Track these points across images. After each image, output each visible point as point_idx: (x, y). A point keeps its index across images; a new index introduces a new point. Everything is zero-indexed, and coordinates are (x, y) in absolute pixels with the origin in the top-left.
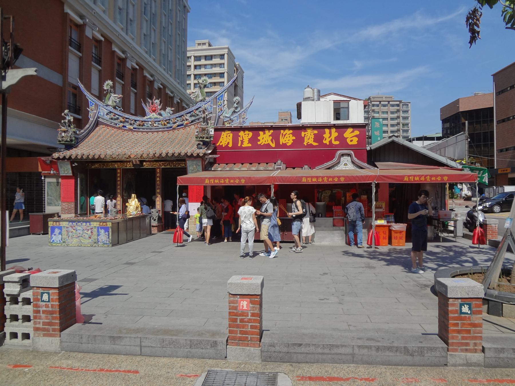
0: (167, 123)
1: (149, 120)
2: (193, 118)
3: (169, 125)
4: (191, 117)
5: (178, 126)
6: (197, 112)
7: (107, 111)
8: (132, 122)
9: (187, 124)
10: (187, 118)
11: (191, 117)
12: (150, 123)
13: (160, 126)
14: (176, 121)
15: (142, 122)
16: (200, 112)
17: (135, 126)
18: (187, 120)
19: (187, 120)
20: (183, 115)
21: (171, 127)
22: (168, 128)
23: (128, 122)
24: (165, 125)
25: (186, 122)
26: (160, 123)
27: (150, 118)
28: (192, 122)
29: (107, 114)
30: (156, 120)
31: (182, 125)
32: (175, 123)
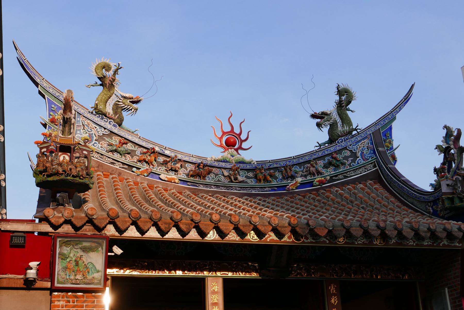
0: (271, 176)
1: (223, 165)
2: (331, 171)
3: (274, 183)
4: (326, 167)
5: (303, 185)
6: (340, 157)
7: (101, 132)
8: (178, 165)
9: (321, 182)
10: (320, 169)
11: (326, 167)
12: (226, 173)
13: (252, 182)
14: (293, 173)
15: (205, 165)
16: (346, 158)
17: (184, 177)
18: (319, 173)
19: (319, 173)
20: (308, 162)
21: (279, 188)
22: (272, 188)
23: (165, 163)
24: (266, 180)
25: (318, 178)
26: (251, 174)
27: (225, 161)
28: (332, 180)
29: (100, 138)
30: (242, 166)
31: (311, 184)
32: (293, 177)
